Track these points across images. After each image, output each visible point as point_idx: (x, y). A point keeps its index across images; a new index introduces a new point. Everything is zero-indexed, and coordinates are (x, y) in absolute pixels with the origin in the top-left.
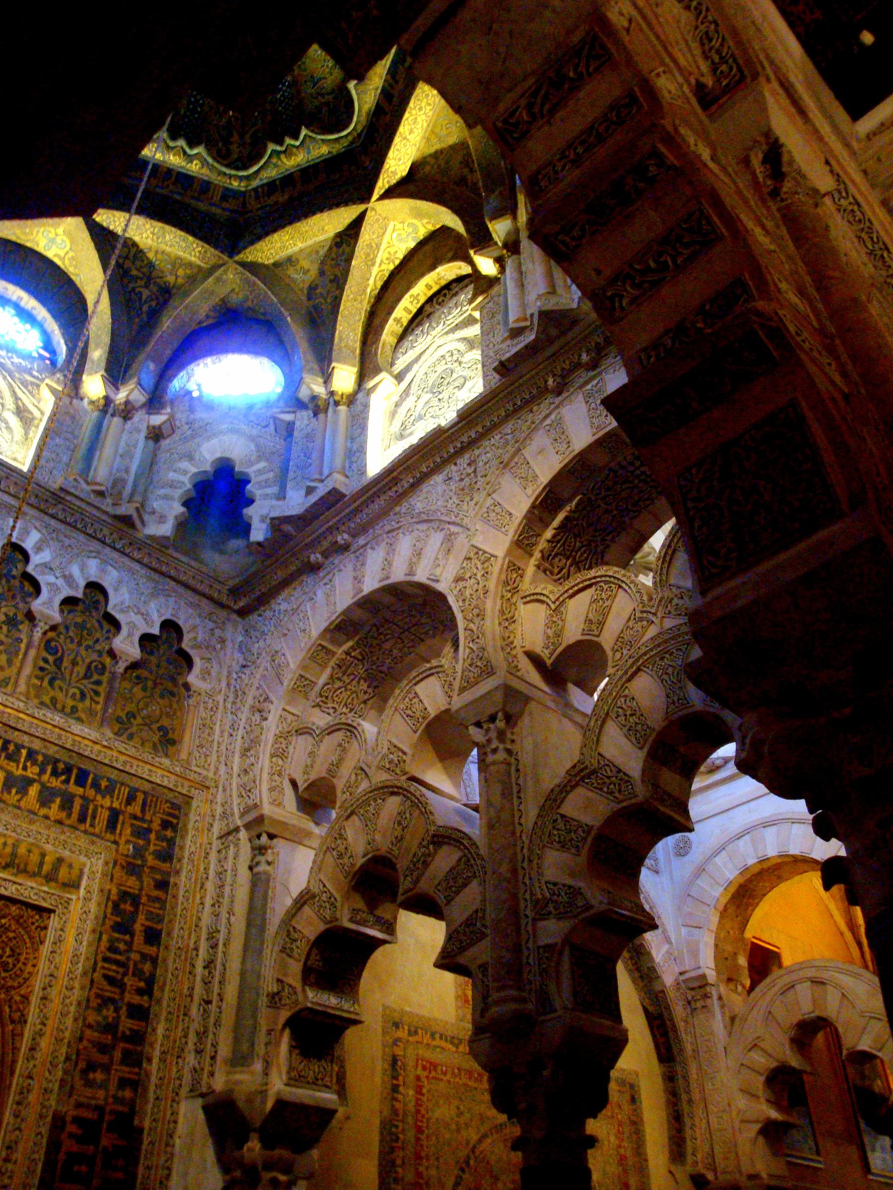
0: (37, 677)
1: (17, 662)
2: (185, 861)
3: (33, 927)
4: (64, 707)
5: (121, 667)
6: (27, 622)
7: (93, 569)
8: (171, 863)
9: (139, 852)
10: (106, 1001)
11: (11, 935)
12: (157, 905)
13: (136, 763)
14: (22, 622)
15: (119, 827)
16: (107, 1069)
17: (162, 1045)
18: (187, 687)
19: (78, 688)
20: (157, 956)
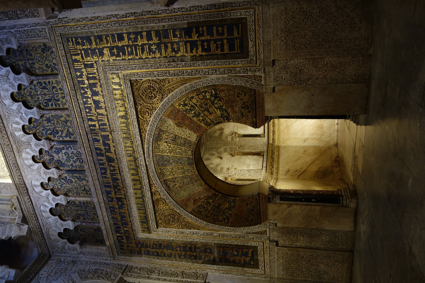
0: (60, 106)
1: (60, 115)
2: (86, 31)
3: (138, 84)
4: (62, 93)
5: (33, 78)
6: (45, 116)
7: (8, 101)
8: (90, 36)
9: (93, 52)
10: (150, 50)
11: (143, 90)
12: (108, 38)
13: (62, 63)
14: (46, 117)
15: (89, 63)
16: (172, 43)
17: (156, 23)
18: (19, 47)
19: (52, 90)
20: (126, 33)
